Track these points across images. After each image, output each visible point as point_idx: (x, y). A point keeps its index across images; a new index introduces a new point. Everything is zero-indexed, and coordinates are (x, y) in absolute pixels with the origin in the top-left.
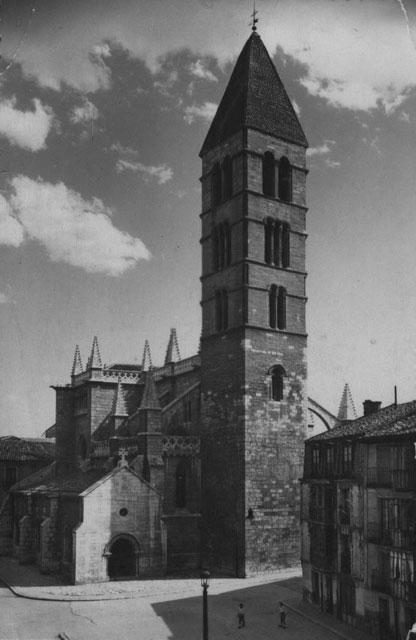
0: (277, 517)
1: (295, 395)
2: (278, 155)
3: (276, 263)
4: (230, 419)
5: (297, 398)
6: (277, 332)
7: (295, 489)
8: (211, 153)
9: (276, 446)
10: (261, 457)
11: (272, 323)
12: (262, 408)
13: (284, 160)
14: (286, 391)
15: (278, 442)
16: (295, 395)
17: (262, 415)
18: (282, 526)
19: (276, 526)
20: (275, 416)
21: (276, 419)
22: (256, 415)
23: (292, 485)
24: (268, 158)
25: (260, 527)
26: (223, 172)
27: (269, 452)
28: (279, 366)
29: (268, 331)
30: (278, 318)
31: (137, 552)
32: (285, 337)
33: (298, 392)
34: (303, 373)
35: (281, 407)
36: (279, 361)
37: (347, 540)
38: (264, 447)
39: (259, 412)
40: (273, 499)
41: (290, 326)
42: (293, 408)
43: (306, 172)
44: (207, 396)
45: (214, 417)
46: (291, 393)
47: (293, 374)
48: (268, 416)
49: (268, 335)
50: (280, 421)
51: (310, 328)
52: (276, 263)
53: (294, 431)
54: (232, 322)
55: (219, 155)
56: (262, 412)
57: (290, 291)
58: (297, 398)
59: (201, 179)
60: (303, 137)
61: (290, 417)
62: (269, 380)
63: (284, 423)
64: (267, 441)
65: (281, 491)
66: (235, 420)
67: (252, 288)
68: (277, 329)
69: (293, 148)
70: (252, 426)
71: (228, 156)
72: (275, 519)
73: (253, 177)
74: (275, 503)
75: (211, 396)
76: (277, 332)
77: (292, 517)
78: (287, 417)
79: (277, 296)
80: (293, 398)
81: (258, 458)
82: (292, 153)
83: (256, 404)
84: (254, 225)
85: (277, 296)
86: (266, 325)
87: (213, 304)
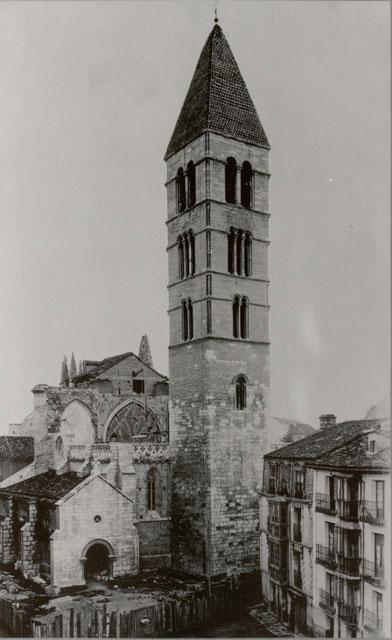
0: (242, 522)
1: (258, 402)
2: (239, 162)
3: (239, 272)
4: (197, 428)
5: (260, 406)
6: (240, 341)
8: (174, 158)
9: (241, 454)
11: (235, 334)
12: (226, 418)
13: (247, 165)
14: (249, 400)
15: (243, 449)
16: (258, 402)
17: (228, 424)
18: (246, 530)
19: (240, 531)
20: (238, 424)
22: (221, 425)
23: (255, 490)
24: (230, 164)
26: (186, 179)
27: (234, 460)
28: (243, 375)
29: (232, 341)
30: (240, 328)
31: (111, 556)
32: (249, 346)
33: (261, 399)
34: (266, 381)
35: (245, 415)
36: (242, 371)
37: (298, 555)
38: (229, 454)
39: (224, 422)
40: (238, 504)
41: (253, 334)
42: (256, 415)
43: (269, 176)
44: (175, 404)
45: (181, 424)
46: (255, 401)
47: (256, 382)
48: (232, 425)
49: (232, 344)
50: (245, 429)
51: (273, 337)
52: (239, 272)
53: (258, 438)
54: (199, 332)
55: (183, 159)
56: (227, 421)
57: (252, 299)
58: (260, 406)
59: (166, 185)
60: (264, 141)
61: (253, 425)
62: (232, 390)
64: (232, 449)
66: (201, 430)
67: (215, 299)
68: (240, 339)
69: (254, 150)
70: (218, 435)
71: (191, 162)
72: (240, 522)
73: (216, 186)
74: (239, 508)
75: (180, 404)
76: (240, 341)
78: (250, 424)
79: (240, 306)
80: (256, 406)
82: (253, 157)
83: (220, 414)
84: (219, 235)
85: (240, 306)
86: (230, 336)
87: (179, 314)
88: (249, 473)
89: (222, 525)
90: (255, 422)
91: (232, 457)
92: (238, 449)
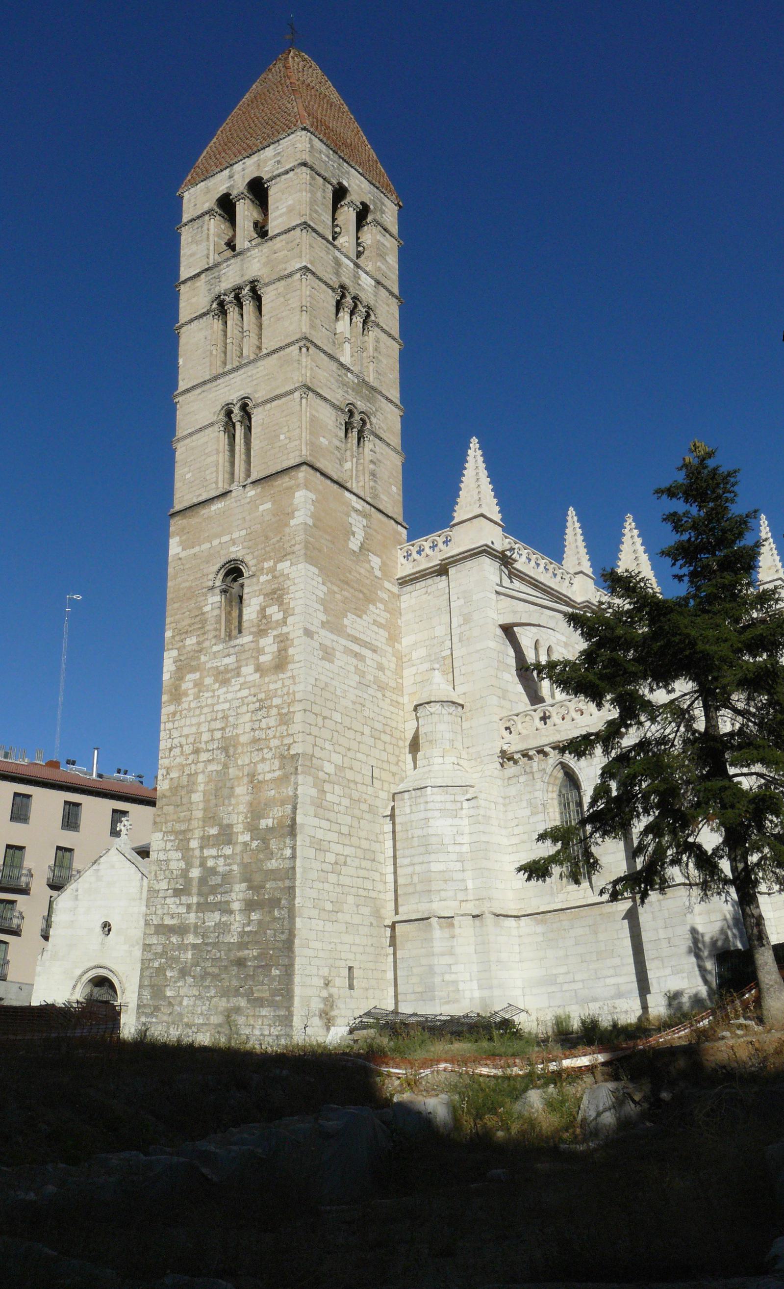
0: (216, 916)
1: (273, 611)
5: (279, 616)
7: (265, 841)
10: (189, 775)
16: (273, 611)
21: (225, 682)
22: (184, 686)
25: (174, 939)
46: (263, 612)
48: (208, 681)
50: (235, 683)
56: (197, 675)
61: (258, 669)
63: (242, 686)
64: (205, 737)
65: (228, 851)
70: (174, 714)
77: (255, 916)
81: (185, 779)
88: (241, 790)
89: (168, 921)
90: (262, 659)
91: (204, 757)
92: (218, 735)
